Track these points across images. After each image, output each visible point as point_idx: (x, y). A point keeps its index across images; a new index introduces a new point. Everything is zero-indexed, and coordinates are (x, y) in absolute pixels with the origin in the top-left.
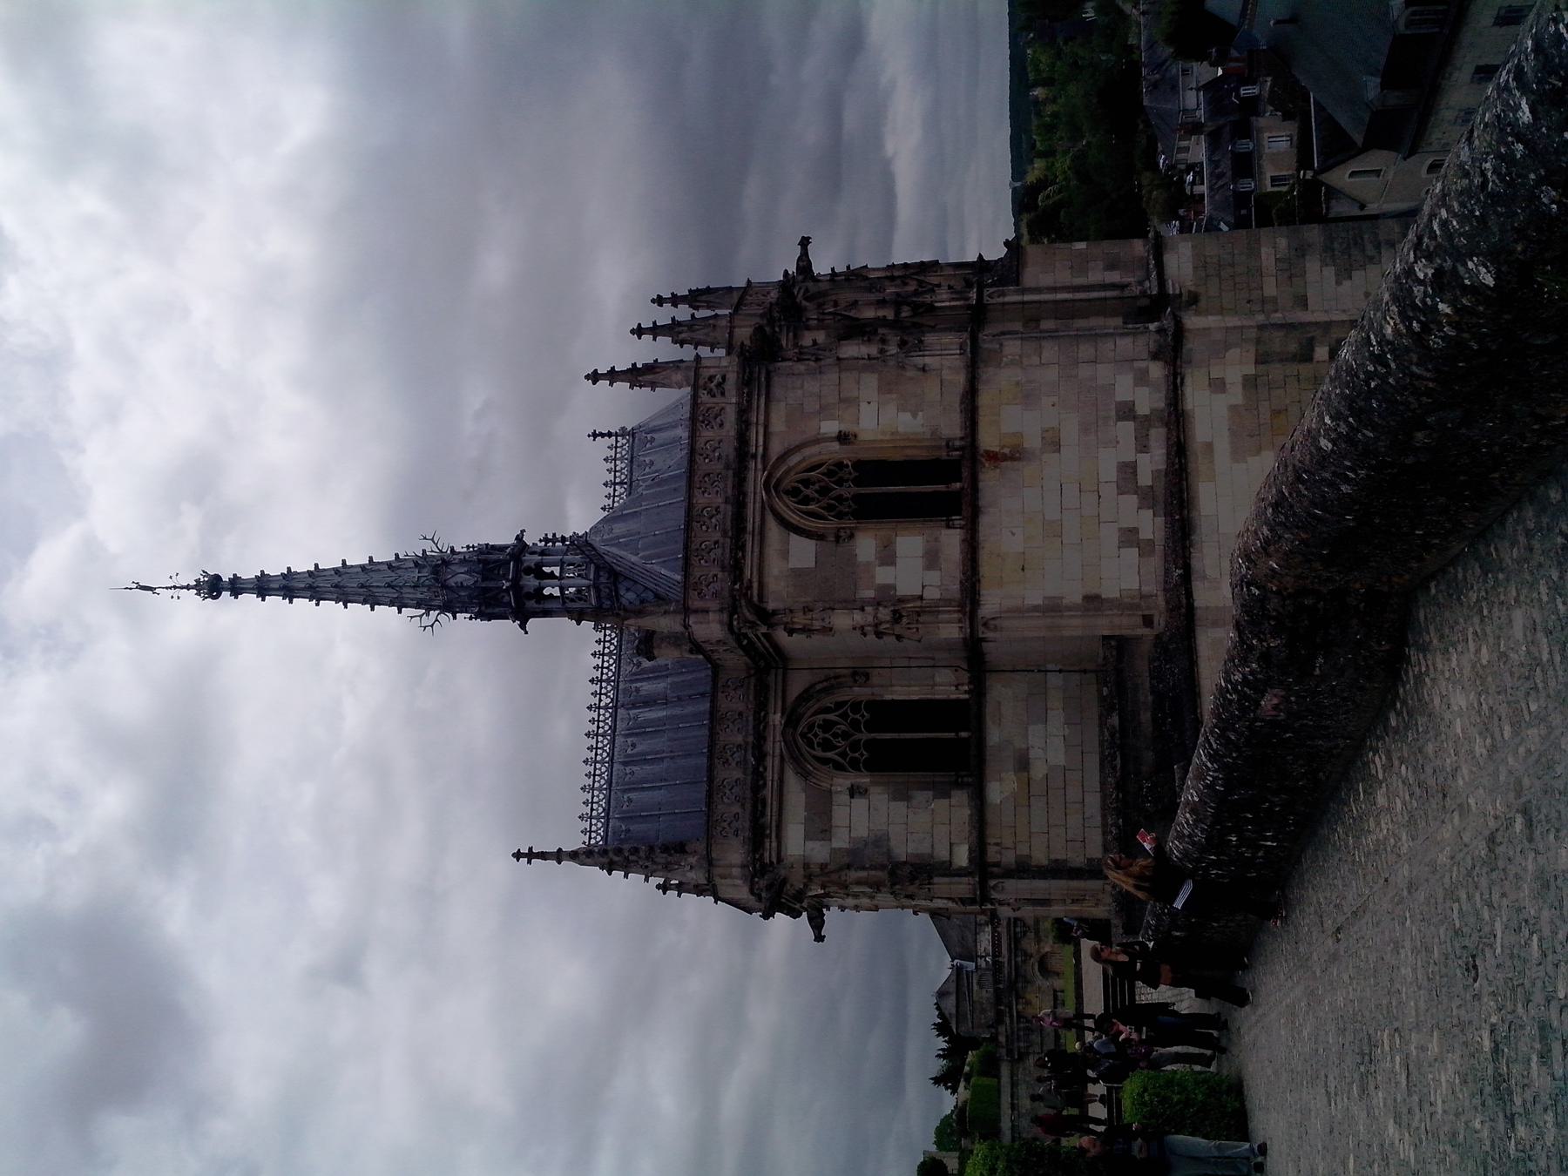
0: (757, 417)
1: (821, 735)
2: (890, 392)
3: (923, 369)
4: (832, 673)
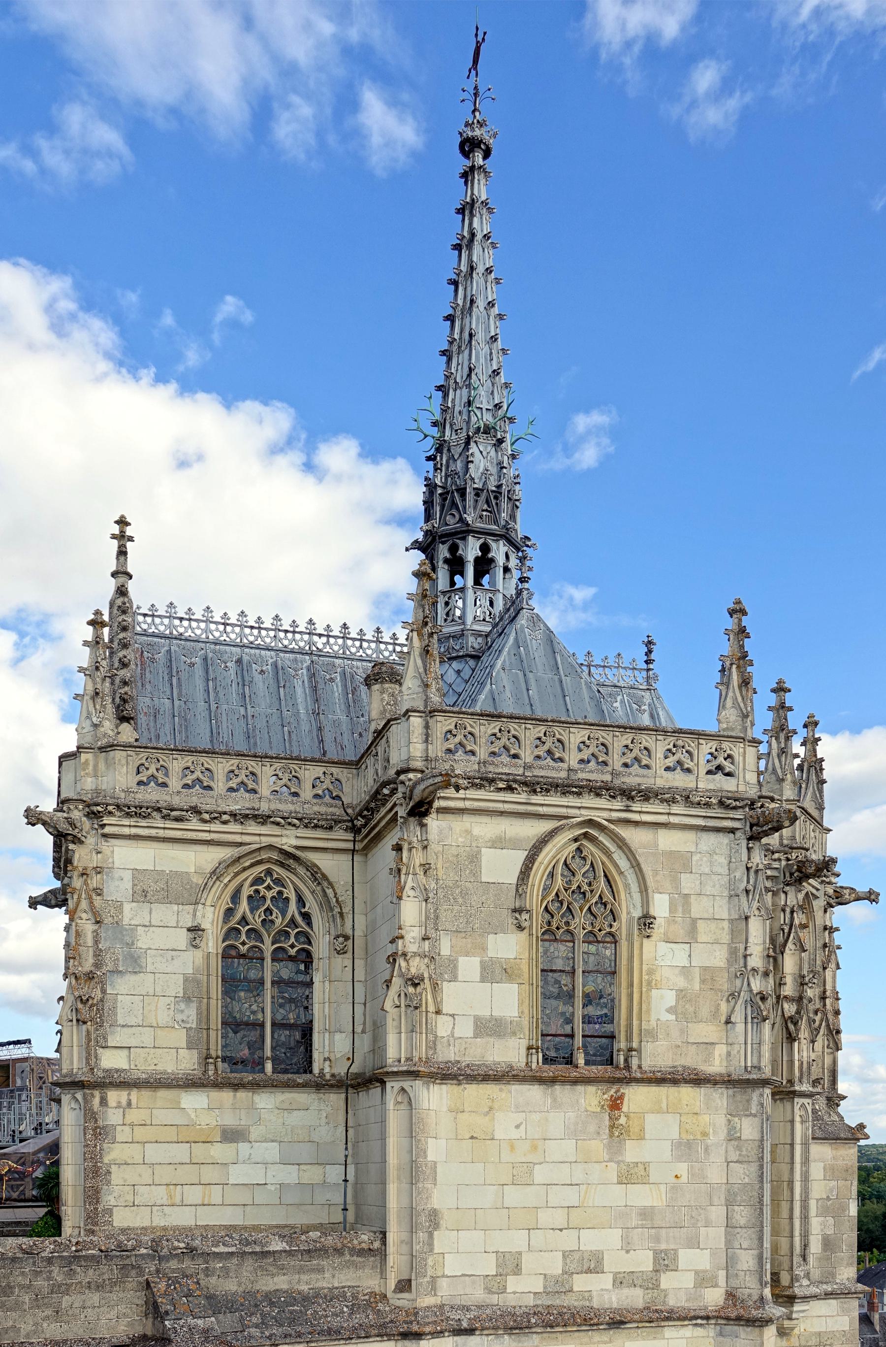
1: (269, 895)
2: (703, 981)
3: (728, 1022)
4: (347, 909)
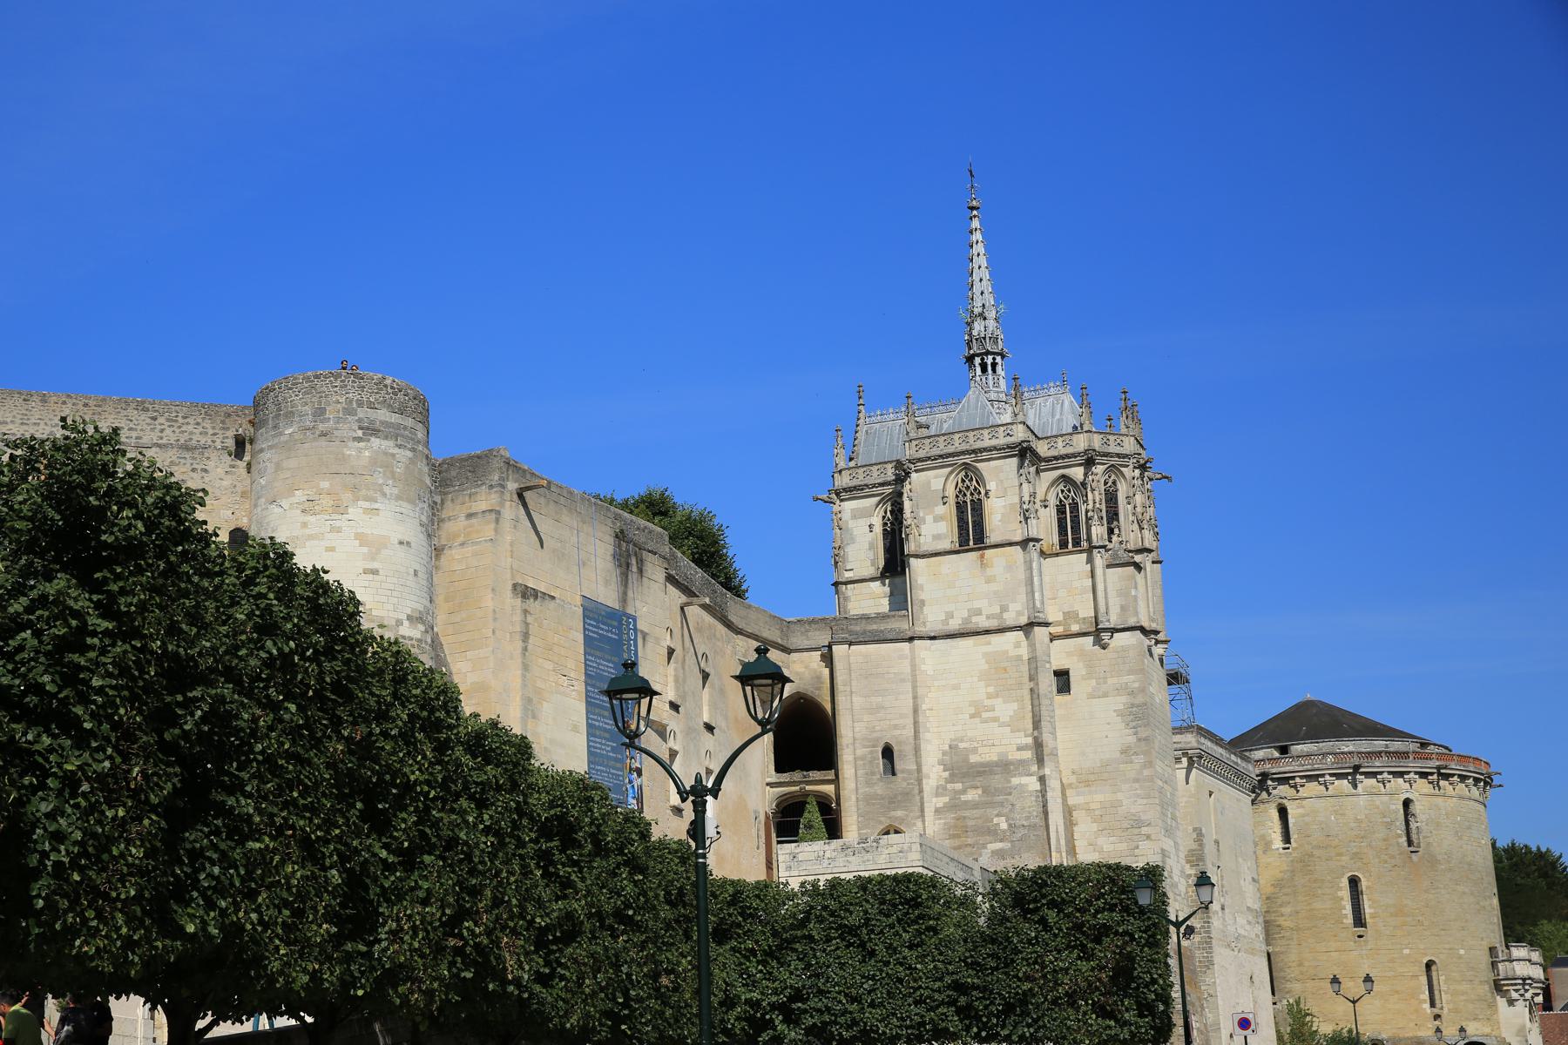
0: (995, 454)
